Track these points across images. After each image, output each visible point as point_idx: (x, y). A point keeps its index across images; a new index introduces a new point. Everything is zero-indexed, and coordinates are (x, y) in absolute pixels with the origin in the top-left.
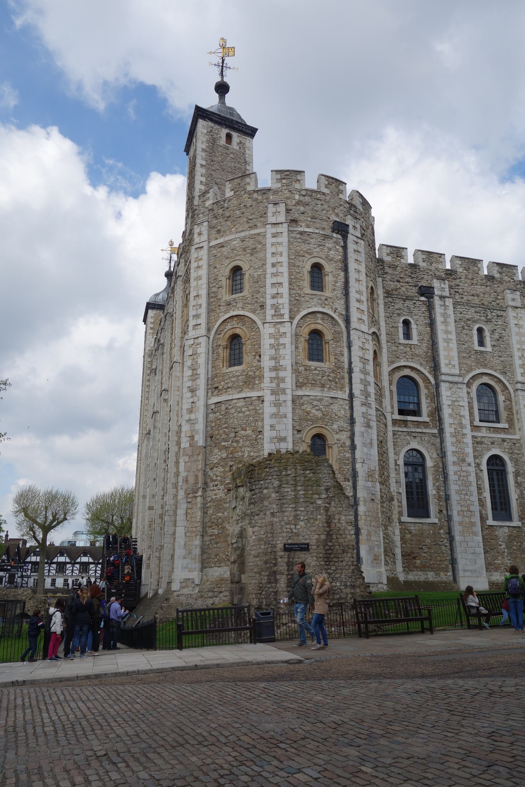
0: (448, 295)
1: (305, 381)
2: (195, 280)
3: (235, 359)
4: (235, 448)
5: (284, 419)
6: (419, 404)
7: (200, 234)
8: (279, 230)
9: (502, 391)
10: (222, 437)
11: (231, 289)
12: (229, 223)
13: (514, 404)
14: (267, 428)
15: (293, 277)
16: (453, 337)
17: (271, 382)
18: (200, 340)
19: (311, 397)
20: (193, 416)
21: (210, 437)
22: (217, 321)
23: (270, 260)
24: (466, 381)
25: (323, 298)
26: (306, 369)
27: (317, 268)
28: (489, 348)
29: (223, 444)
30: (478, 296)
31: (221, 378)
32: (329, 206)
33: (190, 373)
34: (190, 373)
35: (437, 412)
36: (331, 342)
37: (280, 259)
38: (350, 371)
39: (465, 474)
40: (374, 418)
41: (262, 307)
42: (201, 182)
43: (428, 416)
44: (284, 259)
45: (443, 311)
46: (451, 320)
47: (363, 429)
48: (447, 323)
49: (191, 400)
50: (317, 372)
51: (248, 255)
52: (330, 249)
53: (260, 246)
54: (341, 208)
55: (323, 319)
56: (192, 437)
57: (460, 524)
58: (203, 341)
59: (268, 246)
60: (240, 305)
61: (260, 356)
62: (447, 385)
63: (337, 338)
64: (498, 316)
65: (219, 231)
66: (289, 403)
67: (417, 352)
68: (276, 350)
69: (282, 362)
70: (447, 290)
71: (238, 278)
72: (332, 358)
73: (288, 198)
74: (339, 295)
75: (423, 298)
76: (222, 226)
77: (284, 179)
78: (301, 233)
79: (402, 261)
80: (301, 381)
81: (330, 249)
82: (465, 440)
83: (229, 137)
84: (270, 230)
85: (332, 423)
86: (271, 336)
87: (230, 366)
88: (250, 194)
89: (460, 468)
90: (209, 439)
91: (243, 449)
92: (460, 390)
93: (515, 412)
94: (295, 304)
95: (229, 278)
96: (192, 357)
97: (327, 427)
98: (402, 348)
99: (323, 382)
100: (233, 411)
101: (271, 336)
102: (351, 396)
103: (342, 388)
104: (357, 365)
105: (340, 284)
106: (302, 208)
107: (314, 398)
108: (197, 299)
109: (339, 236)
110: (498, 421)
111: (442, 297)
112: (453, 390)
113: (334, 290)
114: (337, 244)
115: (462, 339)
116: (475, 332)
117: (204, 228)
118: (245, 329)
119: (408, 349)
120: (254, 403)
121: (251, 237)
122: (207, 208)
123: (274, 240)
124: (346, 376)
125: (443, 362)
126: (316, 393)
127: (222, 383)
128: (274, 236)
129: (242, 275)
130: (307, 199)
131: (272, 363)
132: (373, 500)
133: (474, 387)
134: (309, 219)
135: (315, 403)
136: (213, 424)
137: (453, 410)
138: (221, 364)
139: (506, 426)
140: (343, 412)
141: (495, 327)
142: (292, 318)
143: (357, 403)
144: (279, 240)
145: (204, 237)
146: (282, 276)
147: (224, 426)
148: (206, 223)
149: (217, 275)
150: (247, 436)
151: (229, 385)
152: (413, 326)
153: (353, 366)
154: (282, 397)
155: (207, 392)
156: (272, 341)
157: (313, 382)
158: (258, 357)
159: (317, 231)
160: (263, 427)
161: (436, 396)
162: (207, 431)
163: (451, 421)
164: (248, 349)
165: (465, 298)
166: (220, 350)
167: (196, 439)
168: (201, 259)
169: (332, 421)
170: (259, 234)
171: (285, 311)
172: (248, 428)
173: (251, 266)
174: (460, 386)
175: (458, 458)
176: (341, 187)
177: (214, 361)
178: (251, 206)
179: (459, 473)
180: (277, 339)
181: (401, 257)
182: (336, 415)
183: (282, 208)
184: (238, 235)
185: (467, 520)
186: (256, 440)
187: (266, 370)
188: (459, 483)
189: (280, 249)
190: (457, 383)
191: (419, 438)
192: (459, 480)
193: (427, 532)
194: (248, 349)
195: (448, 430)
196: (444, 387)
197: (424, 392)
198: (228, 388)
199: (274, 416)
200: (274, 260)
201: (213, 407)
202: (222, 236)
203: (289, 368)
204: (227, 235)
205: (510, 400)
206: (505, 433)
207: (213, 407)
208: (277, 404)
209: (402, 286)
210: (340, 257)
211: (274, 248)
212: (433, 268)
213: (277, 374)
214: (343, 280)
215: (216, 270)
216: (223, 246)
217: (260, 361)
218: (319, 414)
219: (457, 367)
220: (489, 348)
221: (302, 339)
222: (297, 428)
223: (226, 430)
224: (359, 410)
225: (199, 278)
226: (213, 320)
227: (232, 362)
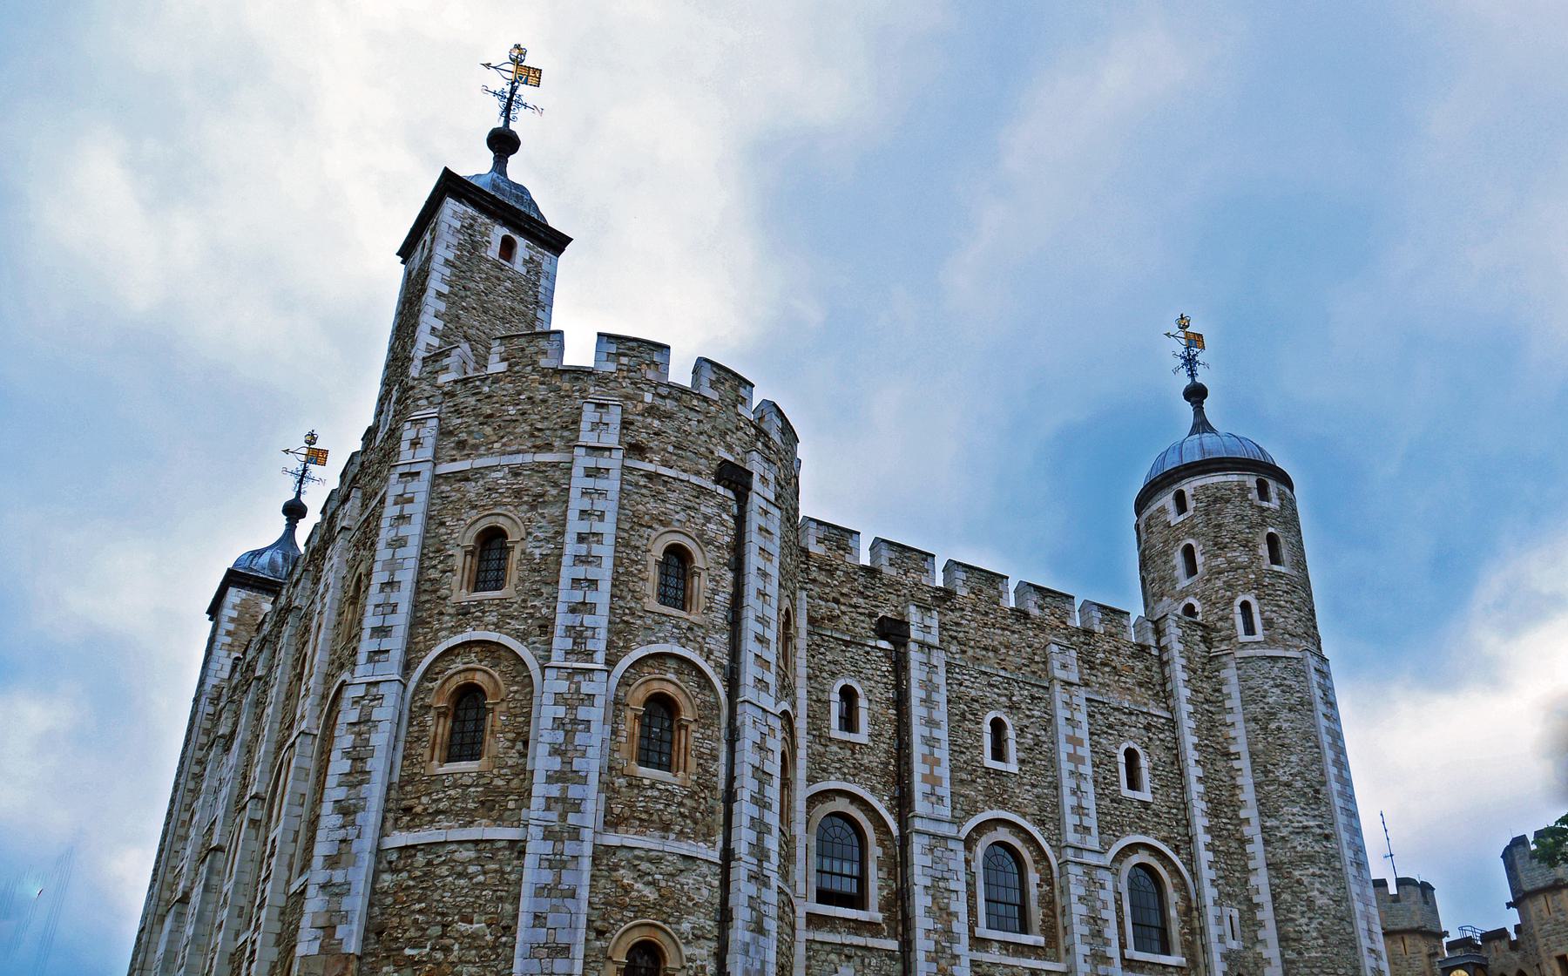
0: (937, 643)
1: (627, 812)
2: (389, 545)
3: (464, 745)
4: (439, 964)
5: (569, 902)
6: (862, 880)
7: (415, 443)
8: (602, 463)
9: (1036, 862)
10: (407, 935)
11: (473, 579)
12: (488, 430)
13: (1057, 892)
14: (524, 919)
15: (621, 570)
16: (943, 734)
17: (548, 809)
18: (383, 689)
19: (636, 852)
20: (338, 876)
21: (374, 930)
22: (430, 648)
23: (575, 525)
24: (963, 835)
25: (684, 625)
26: (630, 785)
27: (677, 556)
28: (1013, 767)
29: (408, 952)
30: (995, 650)
31: (422, 787)
32: (714, 428)
33: (346, 765)
34: (346, 765)
35: (899, 901)
36: (692, 727)
37: (598, 527)
38: (730, 797)
40: (773, 911)
41: (546, 627)
42: (433, 329)
43: (881, 910)
44: (608, 528)
46: (941, 697)
47: (748, 936)
48: (932, 702)
49: (341, 834)
50: (656, 793)
51: (525, 507)
52: (708, 519)
53: (554, 492)
54: (740, 434)
55: (677, 672)
56: (329, 929)
58: (390, 693)
59: (575, 493)
60: (491, 618)
61: (526, 743)
62: (926, 840)
63: (705, 721)
64: (1033, 698)
65: (461, 445)
66: (586, 864)
68: (567, 732)
69: (577, 764)
70: (935, 631)
71: (495, 554)
72: (692, 763)
73: (627, 397)
74: (719, 622)
75: (884, 644)
76: (470, 433)
77: (625, 355)
78: (650, 476)
79: (848, 558)
80: (617, 811)
81: (708, 519)
83: (508, 247)
84: (582, 461)
85: (680, 918)
86: (559, 699)
87: (450, 758)
88: (544, 376)
90: (373, 936)
91: (459, 968)
93: (1059, 911)
94: (621, 633)
95: (472, 553)
96: (356, 729)
97: (667, 927)
98: (835, 748)
99: (667, 817)
100: (444, 871)
101: (559, 699)
102: (728, 855)
103: (707, 837)
104: (747, 786)
105: (723, 598)
106: (656, 423)
107: (642, 854)
108: (388, 590)
109: (730, 494)
110: (1024, 929)
111: (922, 645)
112: (937, 853)
113: (709, 608)
114: (725, 510)
116: (987, 728)
117: (429, 431)
118: (496, 675)
119: (849, 753)
120: (500, 856)
121: (538, 468)
122: (439, 388)
123: (590, 483)
124: (720, 807)
125: (919, 788)
126: (649, 842)
127: (424, 800)
128: (592, 473)
129: (505, 550)
130: (669, 405)
131: (556, 764)
133: (980, 850)
134: (671, 449)
135: (644, 866)
136: (389, 900)
137: (934, 898)
138: (427, 757)
139: (1041, 940)
140: (705, 892)
141: (1026, 722)
142: (611, 662)
143: (740, 872)
144: (601, 484)
145: (426, 452)
146: (599, 566)
147: (417, 907)
148: (435, 422)
149: (444, 543)
150: (474, 936)
151: (441, 806)
152: (862, 703)
153: (736, 785)
154: (569, 848)
155: (384, 819)
156: (561, 711)
157: (644, 816)
158: (519, 746)
159: (684, 476)
160: (516, 917)
161: (899, 864)
162: (370, 917)
163: (929, 924)
164: (498, 723)
165: (970, 652)
166: (429, 719)
167: (338, 935)
168: (411, 501)
169: (681, 911)
170: (555, 465)
171: (599, 646)
172: (476, 917)
173: (529, 534)
174: (951, 844)
176: (743, 392)
177: (409, 744)
178: (544, 401)
180: (571, 708)
181: (847, 549)
182: (690, 899)
183: (614, 417)
184: (505, 460)
186: (494, 948)
187: (539, 777)
189: (600, 505)
190: (946, 838)
194: (498, 723)
195: (923, 945)
196: (918, 844)
197: (875, 851)
198: (438, 812)
199: (542, 891)
200: (584, 527)
201: (394, 857)
202: (468, 455)
203: (594, 779)
204: (481, 456)
205: (1051, 884)
206: (1038, 957)
207: (394, 857)
208: (557, 864)
209: (844, 613)
210: (727, 539)
211: (587, 500)
212: (908, 581)
213: (564, 790)
214: (730, 590)
215: (443, 530)
216: (467, 479)
217: (525, 756)
218: (651, 895)
219: (947, 801)
220: (1013, 767)
221: (630, 714)
222: (598, 924)
223: (421, 918)
224: (743, 889)
225: (399, 543)
226: (422, 645)
227: (456, 749)
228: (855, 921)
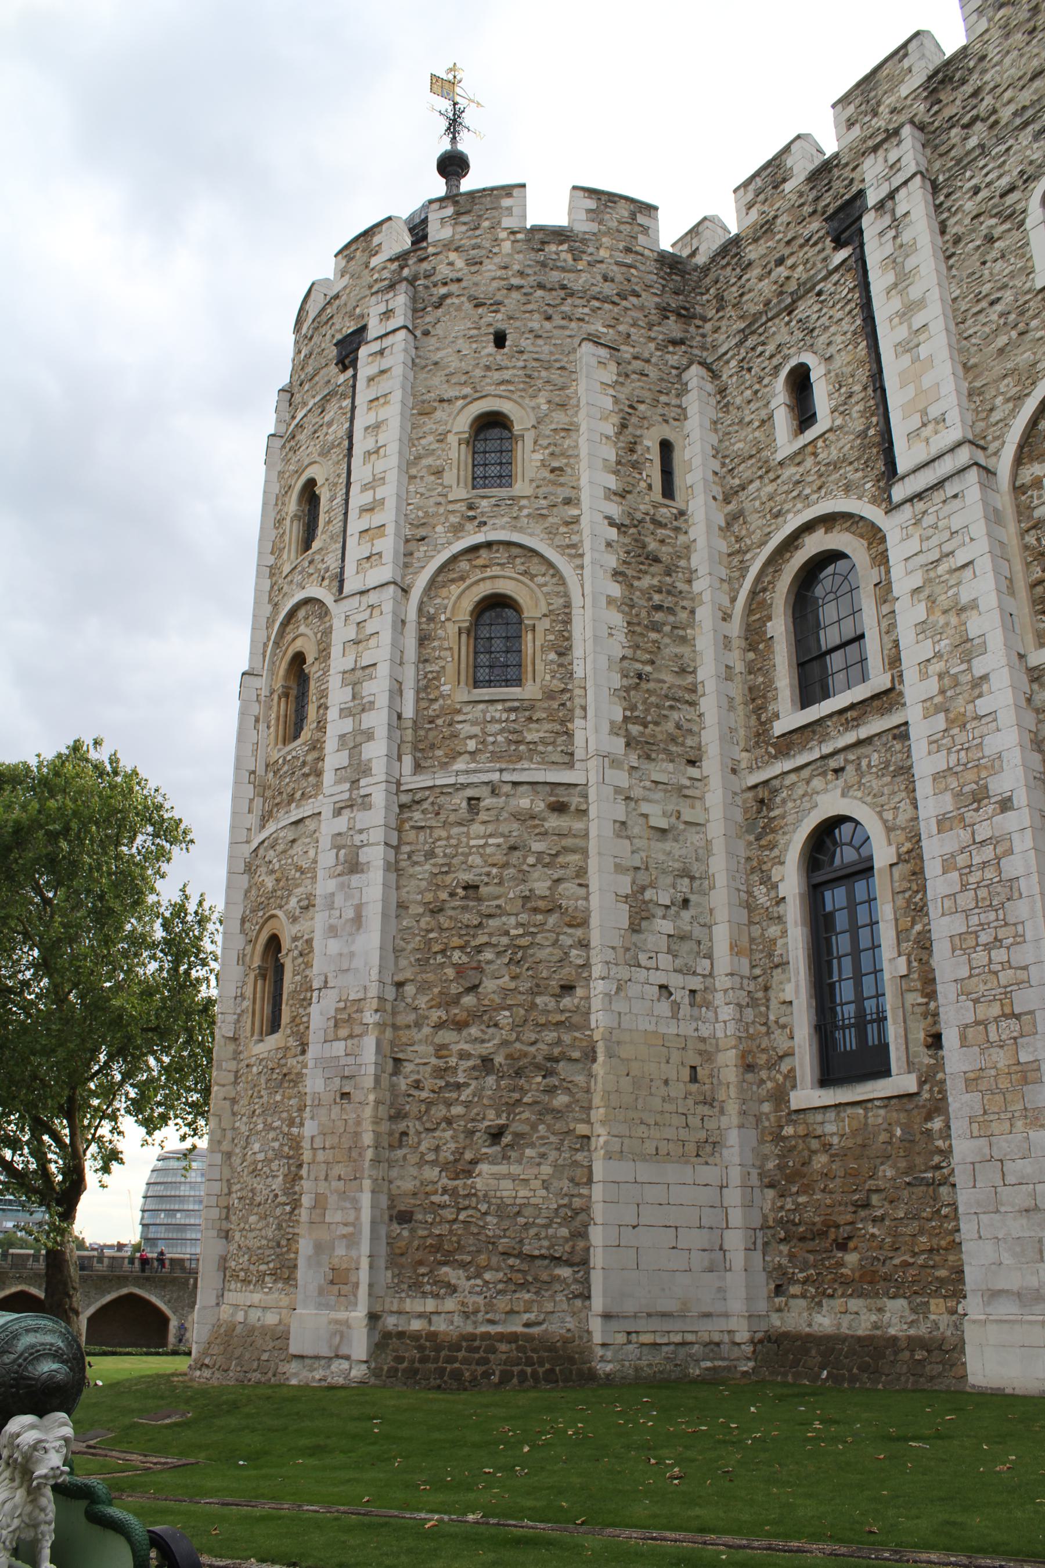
39: (988, 853)
45: (889, 249)
57: (971, 1082)
67: (834, 454)
79: (788, 187)
82: (983, 706)
89: (965, 836)
92: (956, 504)
115: (986, 288)
132: (345, 1095)
174: (950, 489)
175: (958, 795)
179: (962, 860)
185: (1001, 1058)
188: (966, 900)
190: (939, 485)
191: (850, 769)
192: (964, 887)
193: (883, 1137)
209: (793, 267)
228: (852, 707)
